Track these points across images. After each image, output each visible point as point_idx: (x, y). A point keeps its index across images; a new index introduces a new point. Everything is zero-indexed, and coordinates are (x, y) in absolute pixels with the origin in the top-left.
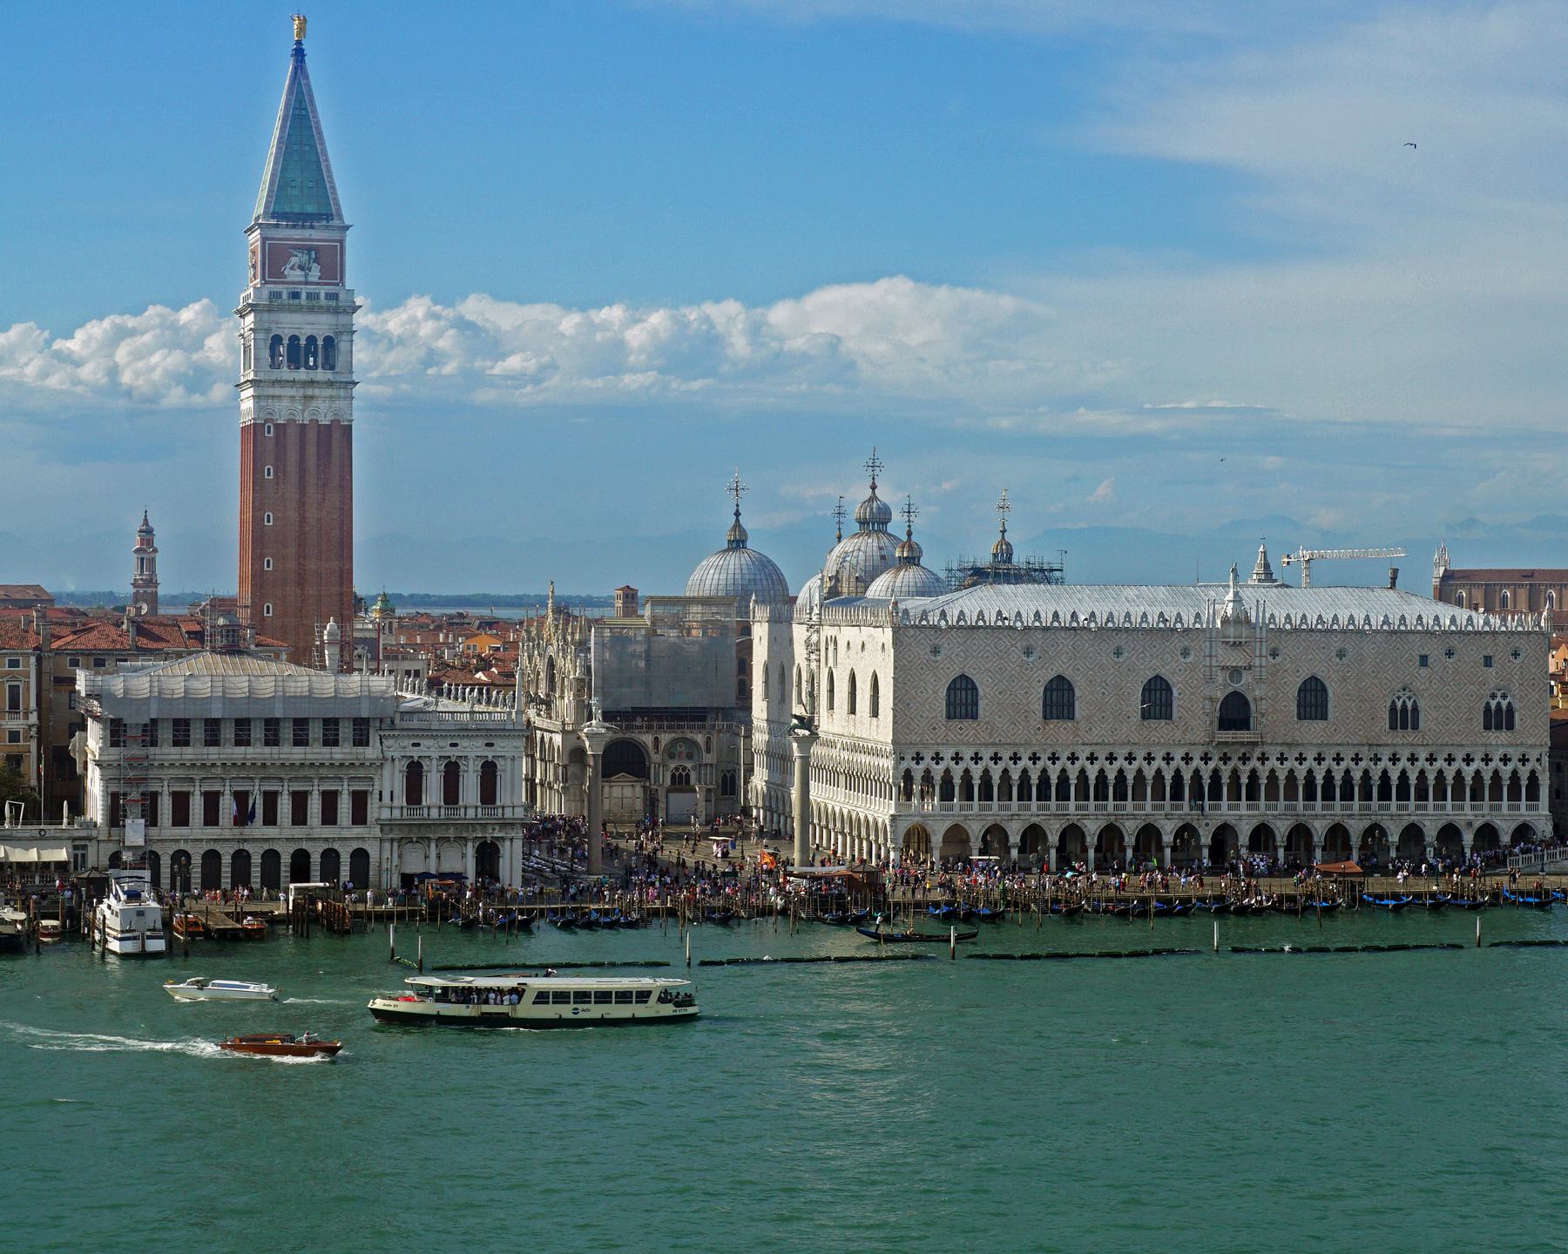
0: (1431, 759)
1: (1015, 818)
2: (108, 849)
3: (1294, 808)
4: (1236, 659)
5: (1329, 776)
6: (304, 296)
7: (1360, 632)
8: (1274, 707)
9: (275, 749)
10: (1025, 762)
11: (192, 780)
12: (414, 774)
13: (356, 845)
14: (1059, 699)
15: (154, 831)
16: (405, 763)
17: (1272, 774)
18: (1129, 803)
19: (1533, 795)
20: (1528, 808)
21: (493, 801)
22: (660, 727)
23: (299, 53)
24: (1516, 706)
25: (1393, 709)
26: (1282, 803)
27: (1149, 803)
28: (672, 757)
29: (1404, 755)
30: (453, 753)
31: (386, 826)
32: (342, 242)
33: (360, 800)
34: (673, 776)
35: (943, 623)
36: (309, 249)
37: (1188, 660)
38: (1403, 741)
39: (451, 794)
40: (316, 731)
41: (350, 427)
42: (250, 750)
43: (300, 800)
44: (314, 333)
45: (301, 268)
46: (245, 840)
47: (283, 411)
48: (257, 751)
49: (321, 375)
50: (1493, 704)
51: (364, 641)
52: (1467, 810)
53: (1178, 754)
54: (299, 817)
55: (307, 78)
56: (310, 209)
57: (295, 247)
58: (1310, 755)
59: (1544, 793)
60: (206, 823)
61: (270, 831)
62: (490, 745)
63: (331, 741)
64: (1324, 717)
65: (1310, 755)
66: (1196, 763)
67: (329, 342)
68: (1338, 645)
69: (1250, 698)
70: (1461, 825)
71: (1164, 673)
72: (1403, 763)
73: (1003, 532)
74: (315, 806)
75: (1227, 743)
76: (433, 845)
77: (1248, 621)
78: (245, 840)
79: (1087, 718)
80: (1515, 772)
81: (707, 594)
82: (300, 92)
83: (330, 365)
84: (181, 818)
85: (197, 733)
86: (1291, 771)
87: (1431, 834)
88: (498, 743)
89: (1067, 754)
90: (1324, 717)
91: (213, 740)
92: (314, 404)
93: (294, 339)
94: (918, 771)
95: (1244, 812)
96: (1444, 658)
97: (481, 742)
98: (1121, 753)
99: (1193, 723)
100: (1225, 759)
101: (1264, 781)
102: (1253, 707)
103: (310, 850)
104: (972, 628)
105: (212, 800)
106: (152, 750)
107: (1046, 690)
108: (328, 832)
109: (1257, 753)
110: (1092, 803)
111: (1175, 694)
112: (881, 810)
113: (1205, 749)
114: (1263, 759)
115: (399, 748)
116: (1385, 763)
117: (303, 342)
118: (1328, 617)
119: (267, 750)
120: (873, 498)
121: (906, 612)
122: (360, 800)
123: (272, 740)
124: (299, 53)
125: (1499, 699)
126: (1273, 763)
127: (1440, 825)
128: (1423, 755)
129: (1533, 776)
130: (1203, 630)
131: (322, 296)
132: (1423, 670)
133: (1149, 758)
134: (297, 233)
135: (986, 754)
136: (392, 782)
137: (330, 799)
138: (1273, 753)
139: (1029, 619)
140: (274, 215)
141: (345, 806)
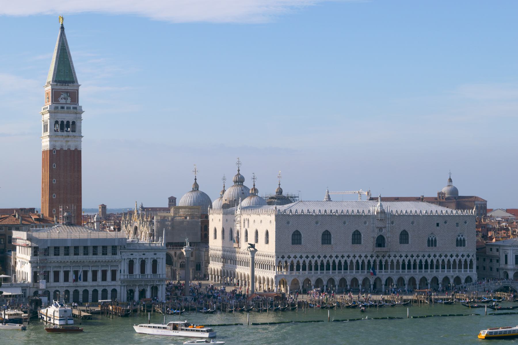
0: (440, 256)
1: (313, 276)
2: (33, 290)
3: (399, 272)
4: (381, 225)
5: (409, 262)
6: (65, 108)
7: (418, 216)
8: (392, 239)
9: (87, 256)
10: (316, 258)
11: (60, 267)
12: (131, 264)
13: (113, 288)
14: (326, 238)
15: (48, 284)
16: (128, 260)
17: (392, 262)
18: (348, 271)
19: (471, 267)
21: (156, 272)
22: (177, 249)
23: (62, 28)
24: (466, 239)
25: (429, 240)
26: (395, 270)
27: (354, 271)
28: (180, 258)
30: (144, 257)
31: (122, 281)
32: (78, 90)
33: (114, 273)
34: (181, 265)
35: (291, 214)
36: (67, 93)
38: (432, 250)
39: (143, 271)
40: (100, 250)
41: (81, 151)
42: (79, 256)
43: (95, 273)
44: (69, 120)
45: (65, 99)
46: (78, 287)
48: (81, 257)
49: (71, 133)
50: (459, 238)
54: (95, 279)
55: (65, 36)
56: (67, 79)
57: (62, 92)
58: (404, 255)
59: (475, 266)
60: (65, 281)
61: (85, 283)
62: (155, 254)
63: (105, 253)
64: (408, 243)
66: (369, 258)
67: (74, 123)
69: (385, 237)
70: (450, 277)
73: (280, 185)
74: (99, 275)
76: (137, 287)
77: (385, 212)
78: (78, 287)
80: (466, 260)
81: (187, 205)
83: (73, 131)
84: (56, 279)
85: (62, 251)
86: (398, 260)
87: (440, 280)
88: (158, 253)
89: (329, 255)
91: (67, 254)
92: (69, 143)
93: (62, 122)
97: (152, 253)
98: (346, 255)
101: (389, 263)
102: (386, 240)
103: (98, 290)
104: (300, 215)
105: (66, 274)
106: (47, 257)
108: (104, 283)
109: (387, 255)
111: (362, 236)
112: (271, 274)
114: (389, 256)
115: (127, 256)
116: (426, 257)
117: (65, 123)
118: (409, 211)
119: (85, 256)
120: (239, 174)
121: (279, 210)
122: (114, 273)
123: (86, 253)
124: (62, 28)
126: (392, 258)
127: (443, 277)
128: (438, 255)
129: (471, 261)
131: (72, 108)
134: (64, 87)
135: (304, 256)
136: (124, 267)
137: (104, 273)
138: (392, 255)
139: (317, 212)
140: (56, 81)
141: (109, 275)
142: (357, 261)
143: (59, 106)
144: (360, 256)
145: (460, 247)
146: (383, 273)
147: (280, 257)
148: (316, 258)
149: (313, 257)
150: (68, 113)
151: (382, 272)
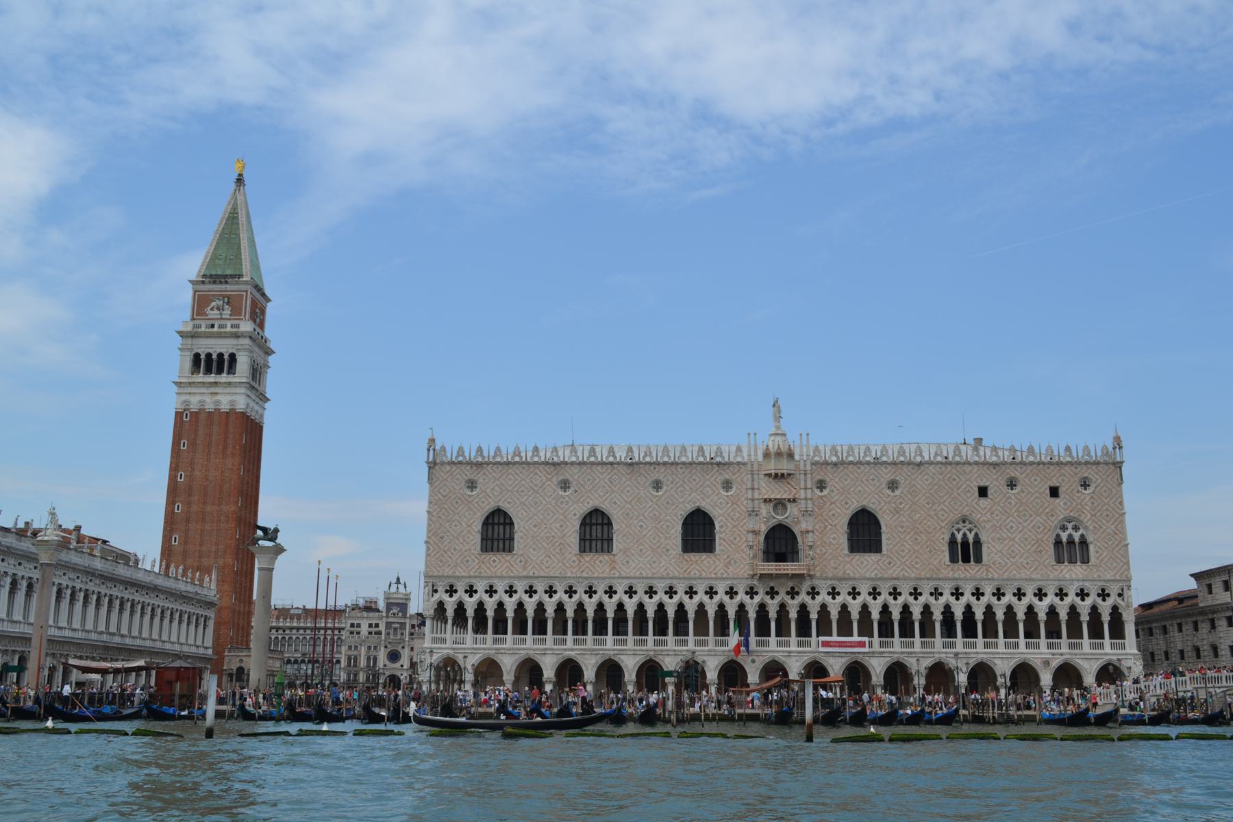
0: (999, 594)
14: (596, 530)
19: (1117, 631)
20: (1113, 647)
24: (1090, 538)
25: (952, 542)
29: (968, 590)
38: (967, 574)
45: (218, 309)
47: (194, 402)
51: (397, 604)
52: (1043, 648)
53: (721, 588)
56: (228, 272)
58: (864, 589)
59: (1130, 629)
64: (878, 549)
65: (864, 589)
66: (741, 597)
68: (889, 477)
69: (796, 530)
70: (1037, 664)
71: (706, 506)
72: (967, 598)
79: (625, 551)
82: (235, 203)
90: (878, 549)
92: (218, 398)
94: (450, 604)
95: (794, 648)
98: (661, 587)
104: (508, 463)
109: (806, 587)
110: (630, 638)
113: (749, 582)
114: (813, 593)
117: (214, 357)
124: (240, 181)
125: (1070, 531)
130: (745, 464)
132: (983, 501)
133: (691, 592)
135: (520, 587)
142: (701, 606)
143: (204, 324)
144: (711, 592)
145: (1071, 566)
146: (794, 648)
147: (441, 589)
148: (560, 595)
150: (220, 336)
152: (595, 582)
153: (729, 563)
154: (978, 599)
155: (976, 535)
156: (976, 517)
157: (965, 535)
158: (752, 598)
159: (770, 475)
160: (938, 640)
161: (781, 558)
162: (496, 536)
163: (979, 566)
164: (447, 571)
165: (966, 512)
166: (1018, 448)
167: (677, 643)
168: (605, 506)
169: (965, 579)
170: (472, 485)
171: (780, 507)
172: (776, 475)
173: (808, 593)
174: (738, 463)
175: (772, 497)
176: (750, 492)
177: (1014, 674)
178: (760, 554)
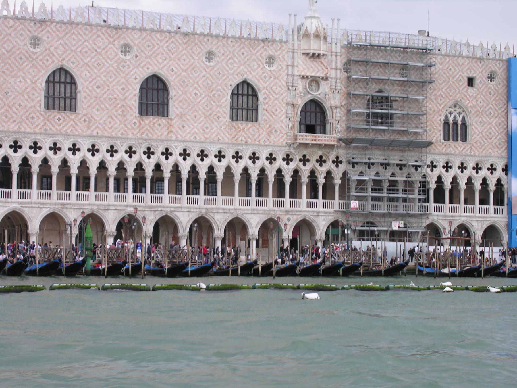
4: (314, 70)
14: (154, 95)
25: (446, 123)
37: (272, 68)
66: (280, 163)
75: (306, 145)
79: (181, 116)
89: (161, 149)
96: (486, 80)
98: (212, 150)
99: (277, 126)
100: (304, 160)
107: (141, 88)
127: (485, 227)
135: (84, 145)
149: (112, 151)
151: (315, 205)
152: (154, 144)
153: (271, 132)
154: (254, 162)
155: (464, 118)
156: (466, 103)
157: (455, 117)
158: (288, 164)
159: (307, 54)
160: (304, 200)
161: (310, 129)
162: (57, 94)
163: (465, 144)
164: (13, 127)
165: (458, 97)
166: (471, 43)
167: (224, 202)
168: (164, 74)
169: (455, 155)
170: (35, 42)
171: (314, 84)
172: (314, 54)
173: (333, 162)
174: (281, 41)
175: (308, 74)
176: (290, 68)
177: (120, 226)
178: (297, 125)
